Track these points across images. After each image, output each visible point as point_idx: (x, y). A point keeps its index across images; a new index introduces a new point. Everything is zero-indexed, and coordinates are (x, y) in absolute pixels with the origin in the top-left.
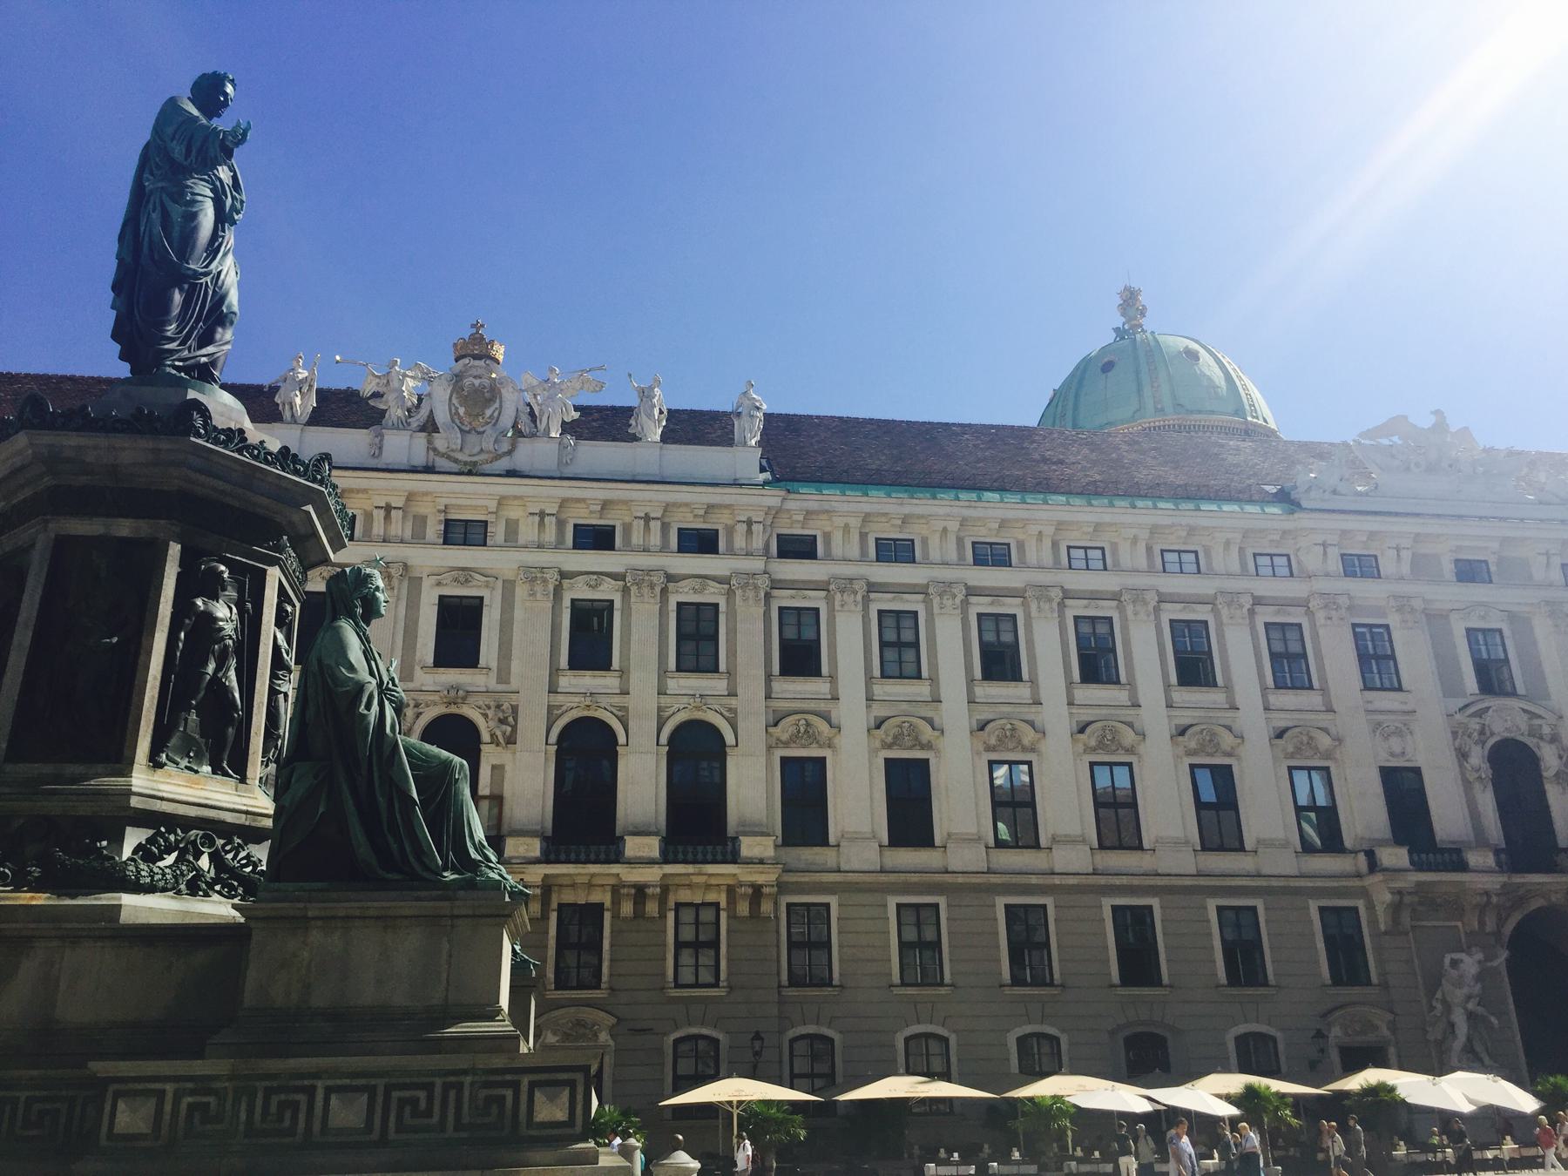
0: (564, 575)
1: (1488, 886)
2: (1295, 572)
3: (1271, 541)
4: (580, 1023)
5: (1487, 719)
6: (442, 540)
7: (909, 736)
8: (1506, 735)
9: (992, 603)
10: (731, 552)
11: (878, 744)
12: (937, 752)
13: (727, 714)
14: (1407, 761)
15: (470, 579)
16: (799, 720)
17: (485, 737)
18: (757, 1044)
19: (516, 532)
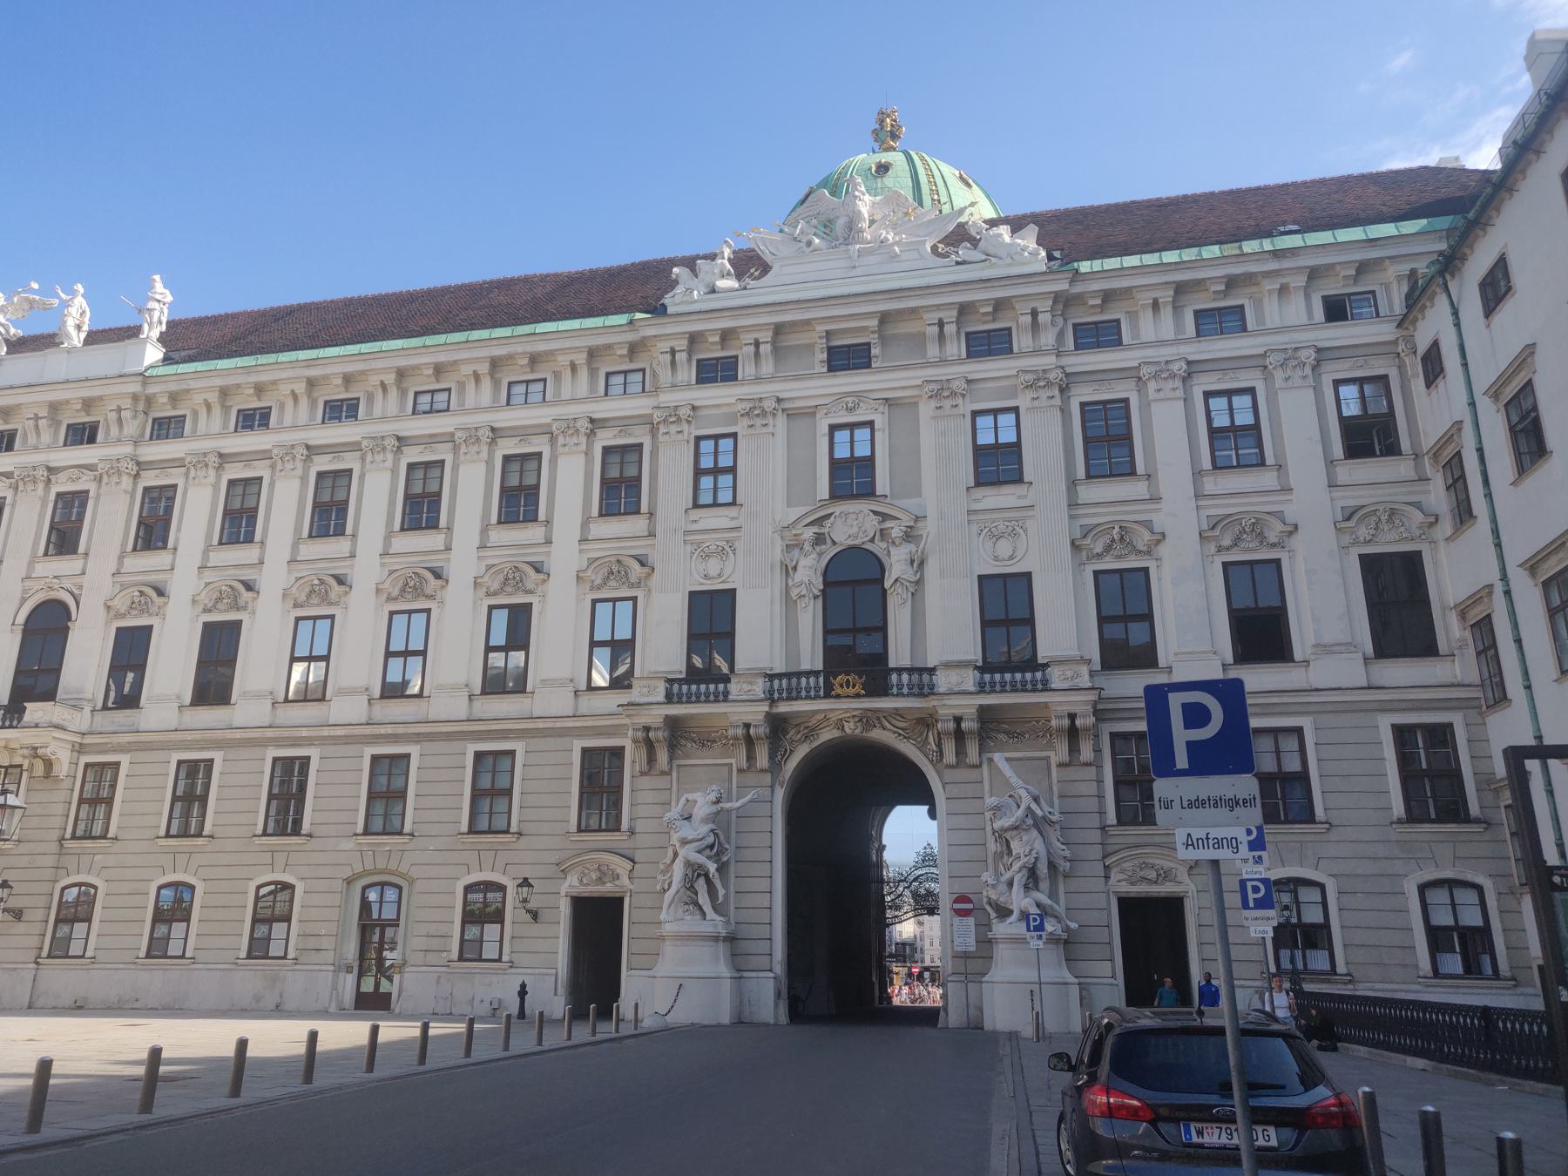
1: (747, 719)
2: (647, 389)
5: (828, 523)
8: (850, 542)
11: (202, 607)
14: (723, 582)
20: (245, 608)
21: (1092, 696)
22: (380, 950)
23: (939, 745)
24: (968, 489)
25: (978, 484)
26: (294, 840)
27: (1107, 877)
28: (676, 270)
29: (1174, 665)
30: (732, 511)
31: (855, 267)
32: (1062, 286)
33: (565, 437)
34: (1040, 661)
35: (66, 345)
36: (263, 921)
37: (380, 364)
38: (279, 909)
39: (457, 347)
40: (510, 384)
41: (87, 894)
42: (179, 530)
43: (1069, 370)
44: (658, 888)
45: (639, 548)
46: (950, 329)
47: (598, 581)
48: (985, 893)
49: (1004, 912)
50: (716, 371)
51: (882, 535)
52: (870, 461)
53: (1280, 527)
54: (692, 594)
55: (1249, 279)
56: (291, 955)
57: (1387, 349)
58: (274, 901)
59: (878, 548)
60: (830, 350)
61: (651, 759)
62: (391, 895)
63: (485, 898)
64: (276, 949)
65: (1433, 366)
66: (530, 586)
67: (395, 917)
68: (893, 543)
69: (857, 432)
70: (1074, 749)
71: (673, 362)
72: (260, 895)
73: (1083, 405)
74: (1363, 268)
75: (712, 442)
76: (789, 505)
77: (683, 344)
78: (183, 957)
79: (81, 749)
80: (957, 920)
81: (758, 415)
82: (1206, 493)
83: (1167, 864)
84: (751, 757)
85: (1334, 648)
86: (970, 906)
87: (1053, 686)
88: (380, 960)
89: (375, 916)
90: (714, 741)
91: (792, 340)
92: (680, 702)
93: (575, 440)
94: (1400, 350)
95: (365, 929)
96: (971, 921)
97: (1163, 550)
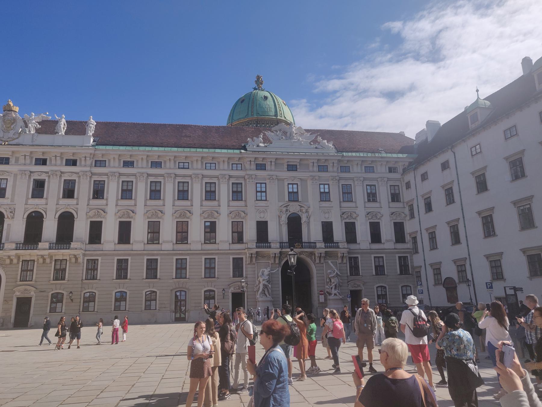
0: (31, 172)
1: (275, 252)
2: (243, 169)
3: (236, 160)
4: (26, 290)
5: (289, 207)
7: (126, 215)
9: (155, 178)
10: (81, 165)
12: (134, 219)
13: (75, 210)
15: (4, 174)
16: (96, 211)
17: (6, 217)
18: (71, 295)
19: (18, 160)
20: (132, 218)
21: (347, 250)
22: (180, 307)
23: (315, 259)
25: (321, 201)
26: (155, 280)
27: (348, 286)
28: (249, 139)
29: (360, 243)
30: (266, 202)
31: (293, 145)
34: (335, 241)
35: (60, 134)
36: (149, 301)
40: (206, 163)
41: (92, 294)
43: (340, 177)
44: (255, 290)
45: (244, 209)
46: (315, 164)
47: (233, 217)
48: (326, 290)
49: (330, 294)
50: (261, 167)
52: (297, 192)
54: (257, 222)
55: (375, 161)
56: (157, 308)
58: (151, 295)
59: (300, 213)
60: (288, 165)
61: (251, 261)
62: (183, 293)
63: (210, 294)
64: (153, 307)
65: (408, 186)
68: (303, 212)
69: (294, 185)
70: (342, 260)
73: (342, 185)
74: (396, 162)
77: (253, 160)
78: (125, 310)
79: (84, 255)
80: (320, 296)
81: (272, 179)
83: (359, 284)
84: (275, 261)
85: (389, 241)
86: (323, 293)
87: (340, 247)
88: (181, 310)
89: (179, 299)
90: (265, 257)
91: (278, 162)
92: (259, 248)
94: (401, 180)
95: (176, 302)
96: (323, 296)
97: (358, 218)
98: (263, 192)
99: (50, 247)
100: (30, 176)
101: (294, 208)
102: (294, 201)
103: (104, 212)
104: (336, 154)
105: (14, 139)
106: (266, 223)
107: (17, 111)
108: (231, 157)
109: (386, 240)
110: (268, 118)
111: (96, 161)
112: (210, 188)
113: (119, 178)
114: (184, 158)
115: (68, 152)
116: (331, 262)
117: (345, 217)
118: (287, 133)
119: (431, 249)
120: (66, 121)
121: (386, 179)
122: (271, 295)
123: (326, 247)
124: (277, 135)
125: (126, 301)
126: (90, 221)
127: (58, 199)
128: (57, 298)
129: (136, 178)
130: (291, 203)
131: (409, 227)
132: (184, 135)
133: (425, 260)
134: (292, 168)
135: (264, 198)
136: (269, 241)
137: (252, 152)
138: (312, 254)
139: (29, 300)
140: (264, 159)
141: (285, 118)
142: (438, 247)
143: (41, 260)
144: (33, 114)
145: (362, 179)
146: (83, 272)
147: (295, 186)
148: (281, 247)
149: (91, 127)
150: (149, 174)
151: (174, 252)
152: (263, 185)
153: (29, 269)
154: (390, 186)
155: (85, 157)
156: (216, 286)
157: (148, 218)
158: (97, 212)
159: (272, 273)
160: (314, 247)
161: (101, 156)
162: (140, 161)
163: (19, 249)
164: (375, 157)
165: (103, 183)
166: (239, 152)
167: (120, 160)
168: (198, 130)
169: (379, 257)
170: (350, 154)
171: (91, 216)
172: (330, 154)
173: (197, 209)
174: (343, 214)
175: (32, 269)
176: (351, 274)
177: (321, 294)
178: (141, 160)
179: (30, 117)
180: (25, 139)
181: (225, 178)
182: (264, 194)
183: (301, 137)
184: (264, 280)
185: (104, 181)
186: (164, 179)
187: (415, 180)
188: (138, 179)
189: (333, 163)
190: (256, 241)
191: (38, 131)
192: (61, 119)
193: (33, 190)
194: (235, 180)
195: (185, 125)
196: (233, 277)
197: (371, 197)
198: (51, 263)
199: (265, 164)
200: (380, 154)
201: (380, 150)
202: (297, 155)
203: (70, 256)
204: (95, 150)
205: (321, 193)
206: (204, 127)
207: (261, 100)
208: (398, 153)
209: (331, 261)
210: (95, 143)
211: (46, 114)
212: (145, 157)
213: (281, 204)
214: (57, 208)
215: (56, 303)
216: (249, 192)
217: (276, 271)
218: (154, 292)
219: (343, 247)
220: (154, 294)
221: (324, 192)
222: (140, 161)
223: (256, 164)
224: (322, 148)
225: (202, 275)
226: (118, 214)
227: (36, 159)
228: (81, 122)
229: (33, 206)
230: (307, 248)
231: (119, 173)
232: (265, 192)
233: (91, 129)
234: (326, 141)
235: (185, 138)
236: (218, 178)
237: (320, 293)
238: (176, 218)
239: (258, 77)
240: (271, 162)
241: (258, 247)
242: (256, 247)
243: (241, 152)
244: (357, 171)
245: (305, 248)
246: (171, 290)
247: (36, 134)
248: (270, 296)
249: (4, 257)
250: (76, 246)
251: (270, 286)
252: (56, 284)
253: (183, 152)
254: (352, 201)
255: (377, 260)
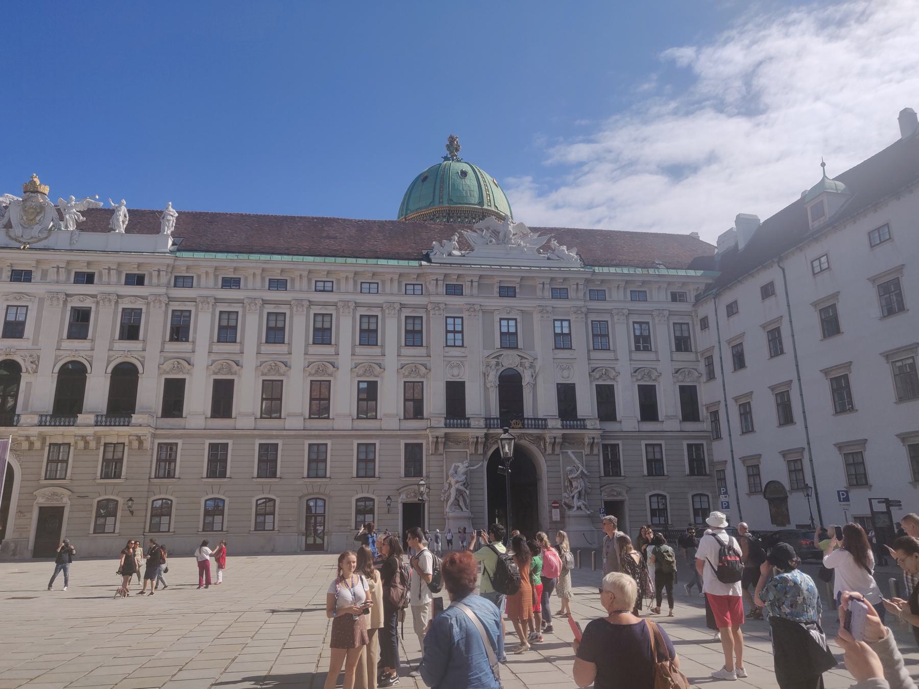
0: (67, 295)
4: (54, 494)
5: (501, 358)
6: (9, 280)
9: (275, 308)
10: (151, 285)
17: (24, 370)
18: (130, 503)
19: (46, 275)
21: (600, 432)
23: (545, 445)
24: (553, 349)
25: (556, 348)
28: (434, 243)
29: (622, 420)
30: (462, 349)
31: (508, 254)
32: (589, 276)
33: (389, 310)
34: (579, 417)
35: (117, 231)
37: (302, 267)
38: (268, 510)
39: (340, 264)
40: (362, 283)
41: (167, 503)
42: (195, 332)
45: (424, 360)
46: (547, 286)
47: (407, 374)
49: (570, 507)
50: (454, 290)
51: (521, 364)
52: (516, 334)
53: (656, 374)
54: (447, 382)
55: (649, 282)
56: (276, 529)
57: (688, 314)
58: (266, 506)
59: (520, 369)
60: (500, 287)
61: (436, 448)
62: (320, 503)
63: (365, 504)
64: (268, 526)
65: (704, 323)
66: (376, 373)
67: (323, 512)
68: (525, 368)
69: (510, 322)
70: (592, 449)
71: (437, 284)
72: (258, 503)
73: (592, 321)
74: (684, 284)
75: (453, 319)
76: (484, 349)
77: (442, 277)
78: (222, 530)
79: (154, 436)
80: (553, 510)
81: (472, 311)
82: (633, 359)
83: (619, 490)
84: (476, 450)
85: (672, 417)
86: (558, 505)
87: (588, 427)
88: (316, 531)
90: (460, 442)
92: (450, 427)
93: (393, 312)
95: (308, 518)
96: (558, 510)
97: (619, 379)
98: (458, 332)
99: (97, 422)
100: (65, 302)
101: (510, 360)
102: (510, 348)
103: (189, 364)
104: (581, 269)
105: (40, 240)
106: (462, 384)
107: (47, 192)
108: (404, 273)
109: (666, 416)
110: (468, 208)
111: (176, 277)
112: (369, 325)
113: (214, 306)
114: (326, 273)
115: (129, 263)
116: (572, 452)
117: (597, 377)
118: (499, 233)
119: (743, 433)
120: (129, 211)
121: (666, 313)
122: (469, 509)
123: (564, 427)
124: (482, 237)
125: (223, 515)
126: (165, 379)
127: (112, 341)
128: (107, 509)
129: (244, 307)
130: (505, 352)
131: (706, 395)
132: (325, 234)
133: (732, 451)
134: (507, 292)
135: (459, 343)
136: (467, 416)
137: (439, 265)
138: (540, 438)
139: (60, 510)
140: (459, 276)
141: (497, 207)
142: (755, 429)
143: (81, 444)
144: (74, 198)
145: (626, 312)
146: (151, 465)
147: (512, 323)
148: (488, 426)
149: (169, 221)
150: (266, 300)
151: (306, 433)
152: (458, 321)
153: (60, 459)
154: (674, 324)
155: (159, 271)
156: (376, 491)
157: (263, 374)
158: (177, 363)
159: (471, 471)
160: (544, 427)
161: (185, 268)
162: (251, 278)
163: (45, 425)
164: (649, 275)
165: (187, 314)
166: (417, 265)
167: (216, 276)
168: (349, 227)
169: (653, 445)
170: (606, 270)
171: (167, 370)
172: (571, 269)
173: (345, 360)
174: (593, 371)
175: (65, 458)
176: (607, 474)
177: (556, 507)
178: (252, 276)
179: (68, 203)
180: (59, 240)
181: (394, 308)
182: (459, 336)
183: (522, 240)
184: (457, 482)
185: (190, 311)
186: (291, 309)
187: (716, 315)
188: (247, 309)
189: (577, 284)
190: (445, 416)
191: (80, 226)
192: (120, 206)
193: (70, 325)
194: (410, 312)
195: (327, 218)
196: (405, 477)
197: (641, 342)
198: (97, 449)
199: (462, 285)
200: (656, 270)
201: (657, 262)
202: (515, 271)
203: (131, 438)
204: (175, 260)
205: (556, 335)
206: (359, 223)
207: (456, 178)
208: (689, 268)
209: (572, 451)
210: (175, 247)
211: (93, 198)
212: (258, 272)
213: (487, 353)
214: (109, 357)
215: (105, 517)
216: (435, 331)
217: (478, 468)
218: (271, 500)
219: (593, 428)
220: (271, 503)
221: (562, 334)
222: (251, 278)
223: (446, 285)
224: (558, 259)
225: (352, 473)
226: (213, 367)
227: (76, 273)
228: (153, 212)
229: (70, 352)
230: (532, 428)
231: (215, 299)
232: (462, 332)
233: (169, 224)
234: (564, 248)
235: (327, 241)
236: (382, 308)
237: (553, 505)
238: (310, 374)
239: (452, 139)
240: (472, 281)
241: (448, 426)
242: (444, 426)
243: (421, 265)
244: (617, 298)
245: (528, 428)
246: (300, 498)
247: (77, 232)
248: (468, 509)
249: (19, 438)
250: (140, 421)
251: (468, 492)
252: (105, 485)
253: (324, 264)
254: (609, 349)
255: (650, 449)
